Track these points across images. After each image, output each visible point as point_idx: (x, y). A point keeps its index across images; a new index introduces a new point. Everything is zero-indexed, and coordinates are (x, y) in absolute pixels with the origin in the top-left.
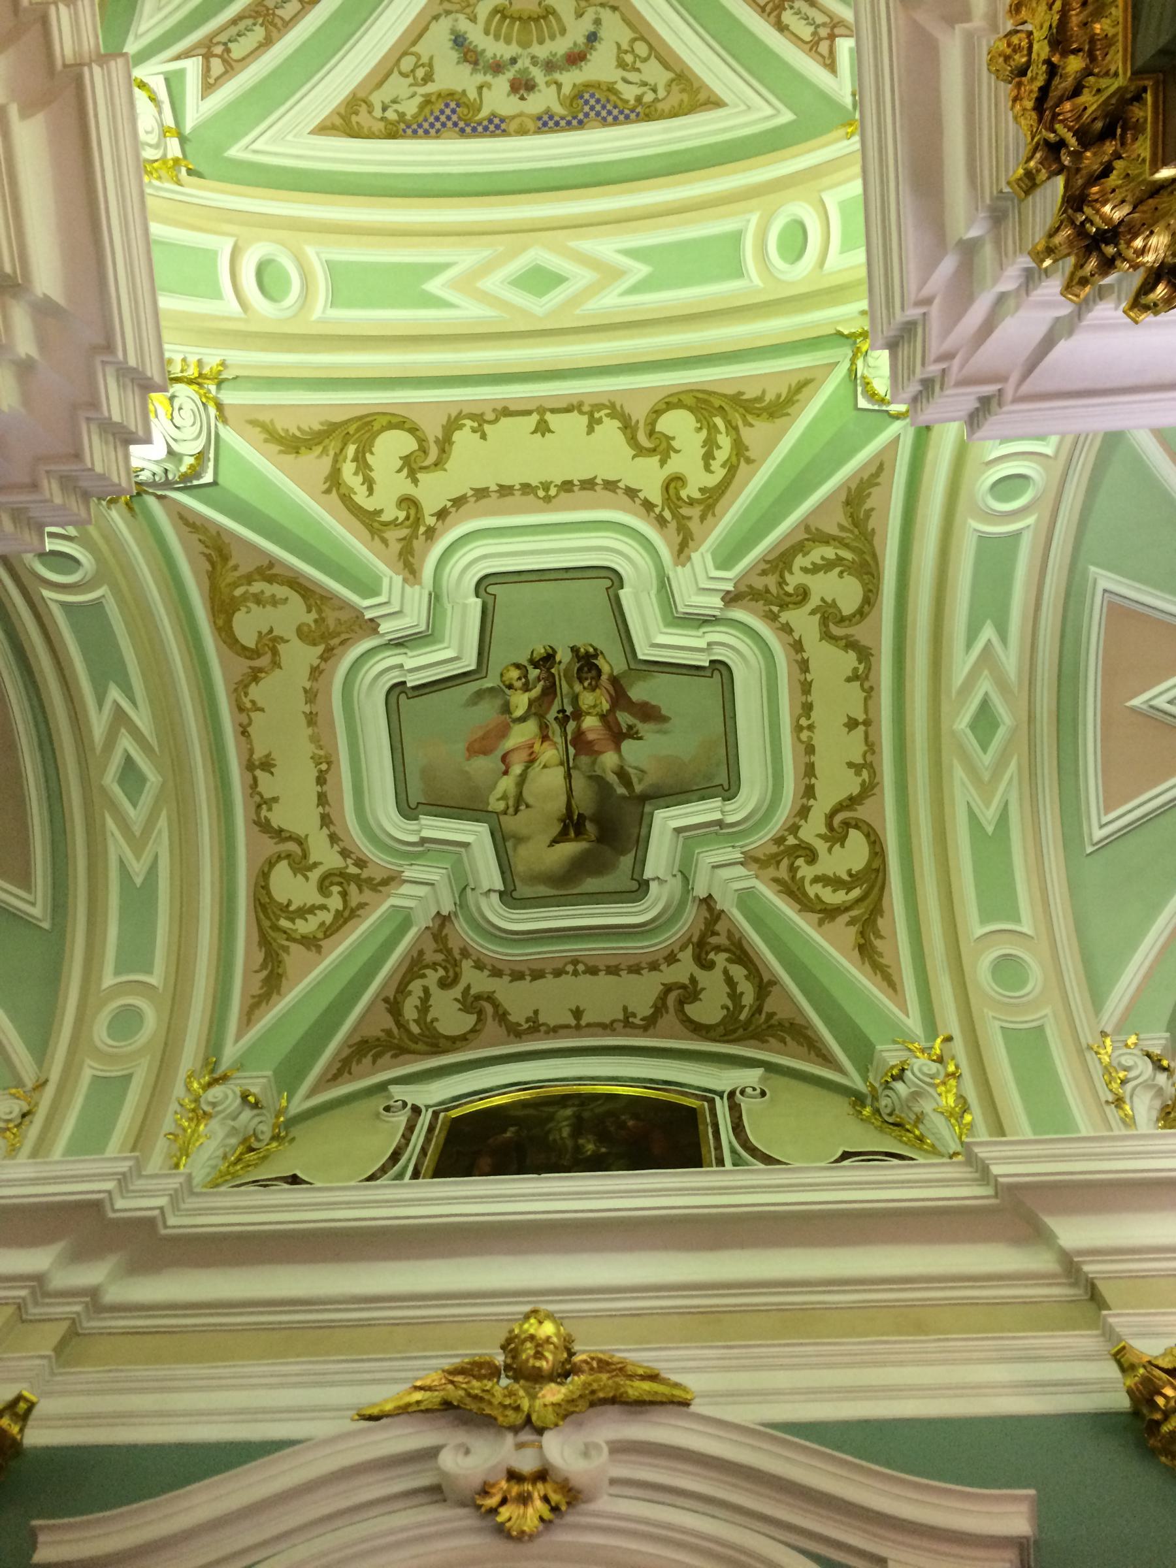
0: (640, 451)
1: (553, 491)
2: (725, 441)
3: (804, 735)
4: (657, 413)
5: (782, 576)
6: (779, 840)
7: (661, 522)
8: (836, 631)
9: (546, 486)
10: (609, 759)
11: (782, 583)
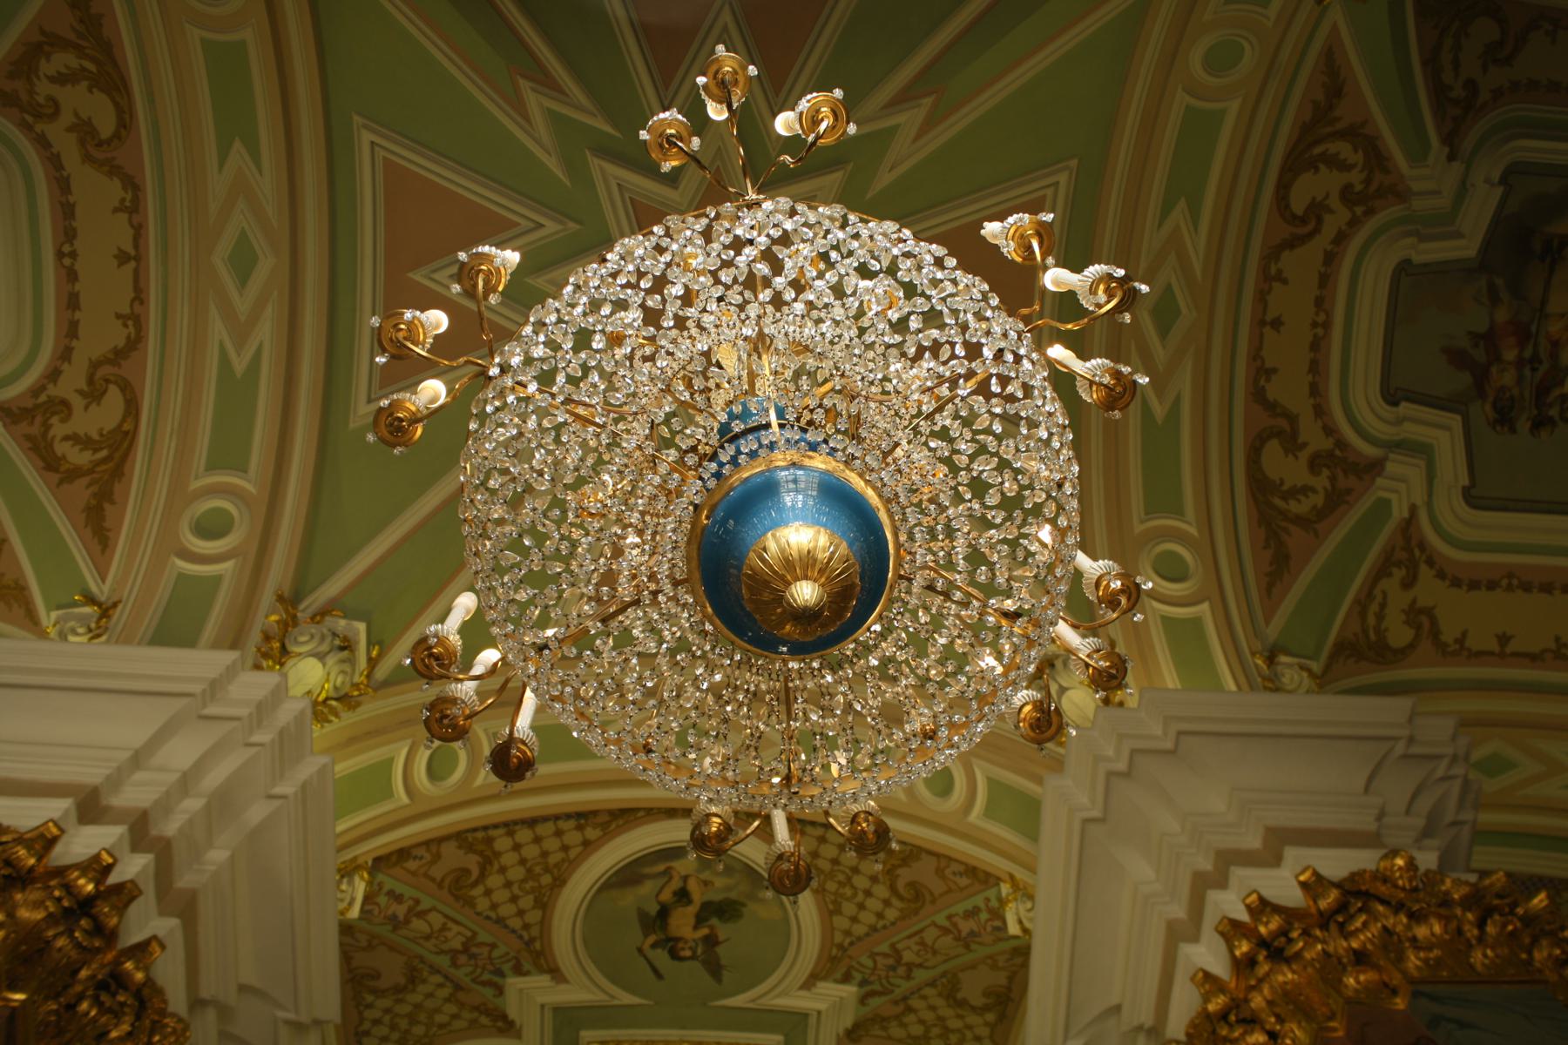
0: (1429, 612)
1: (1504, 582)
2: (1371, 620)
3: (1321, 318)
4: (1412, 646)
5: (1333, 486)
6: (1370, 212)
7: (1422, 546)
8: (1283, 423)
9: (1510, 588)
10: (1502, 315)
11: (1333, 479)
